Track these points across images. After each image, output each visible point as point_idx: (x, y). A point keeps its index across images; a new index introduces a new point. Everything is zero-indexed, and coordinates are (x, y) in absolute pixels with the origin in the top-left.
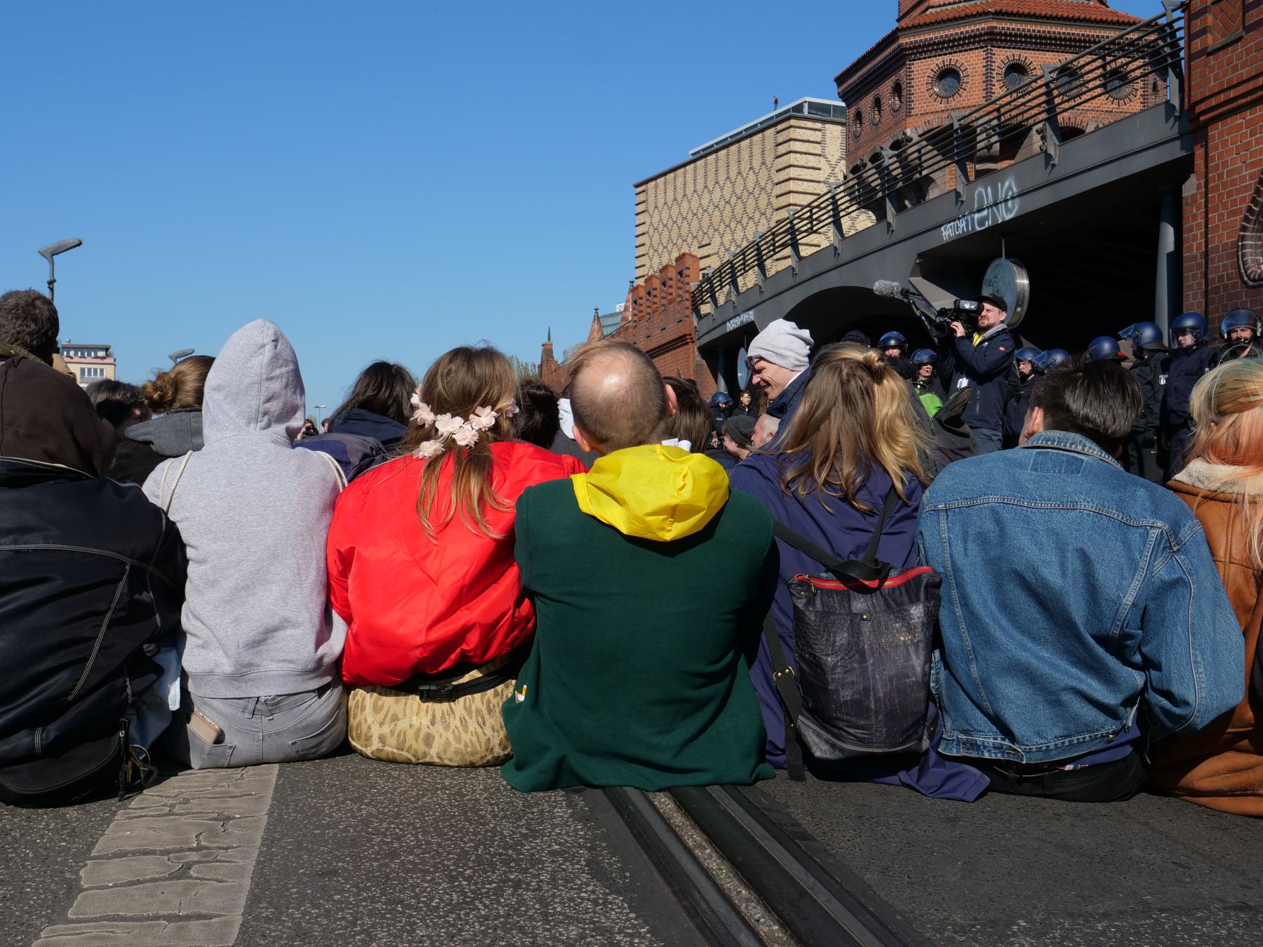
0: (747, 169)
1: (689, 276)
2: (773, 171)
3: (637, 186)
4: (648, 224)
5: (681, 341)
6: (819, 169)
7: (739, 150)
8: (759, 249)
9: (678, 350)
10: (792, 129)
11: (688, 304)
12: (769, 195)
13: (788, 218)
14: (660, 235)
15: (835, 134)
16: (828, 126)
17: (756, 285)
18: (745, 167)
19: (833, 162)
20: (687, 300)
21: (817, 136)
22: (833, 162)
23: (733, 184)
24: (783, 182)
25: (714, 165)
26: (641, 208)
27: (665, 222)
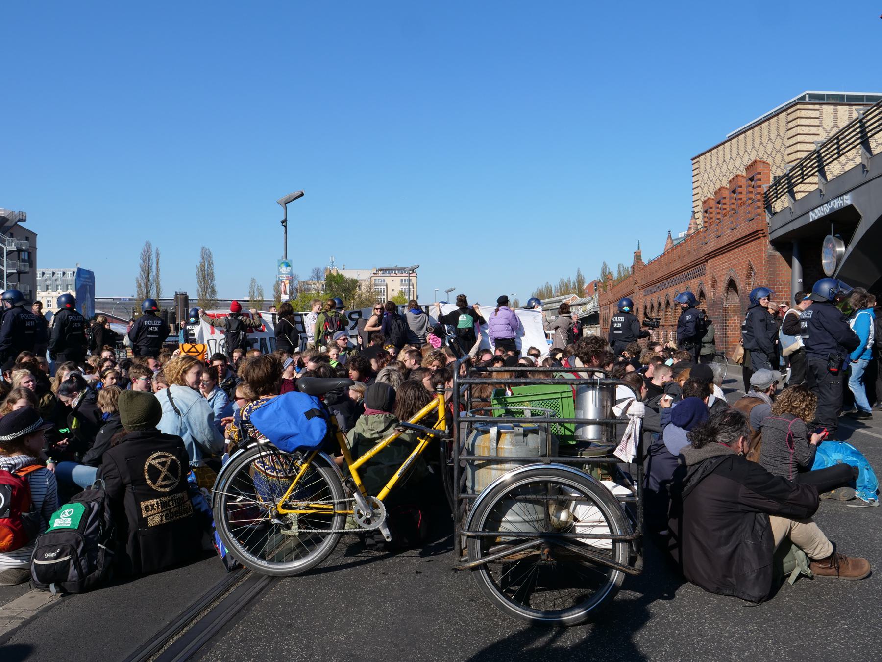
0: (767, 140)
1: (760, 180)
2: (785, 139)
3: (693, 160)
4: (700, 181)
5: (754, 236)
6: (818, 135)
7: (761, 129)
8: (819, 156)
9: (749, 245)
10: (798, 111)
11: (760, 204)
12: (782, 155)
13: (857, 118)
14: (708, 187)
15: (829, 111)
16: (824, 107)
17: (861, 164)
18: (765, 139)
19: (828, 130)
20: (759, 200)
21: (816, 114)
22: (828, 130)
23: (757, 151)
24: (793, 145)
25: (744, 141)
26: (696, 172)
27: (711, 179)
